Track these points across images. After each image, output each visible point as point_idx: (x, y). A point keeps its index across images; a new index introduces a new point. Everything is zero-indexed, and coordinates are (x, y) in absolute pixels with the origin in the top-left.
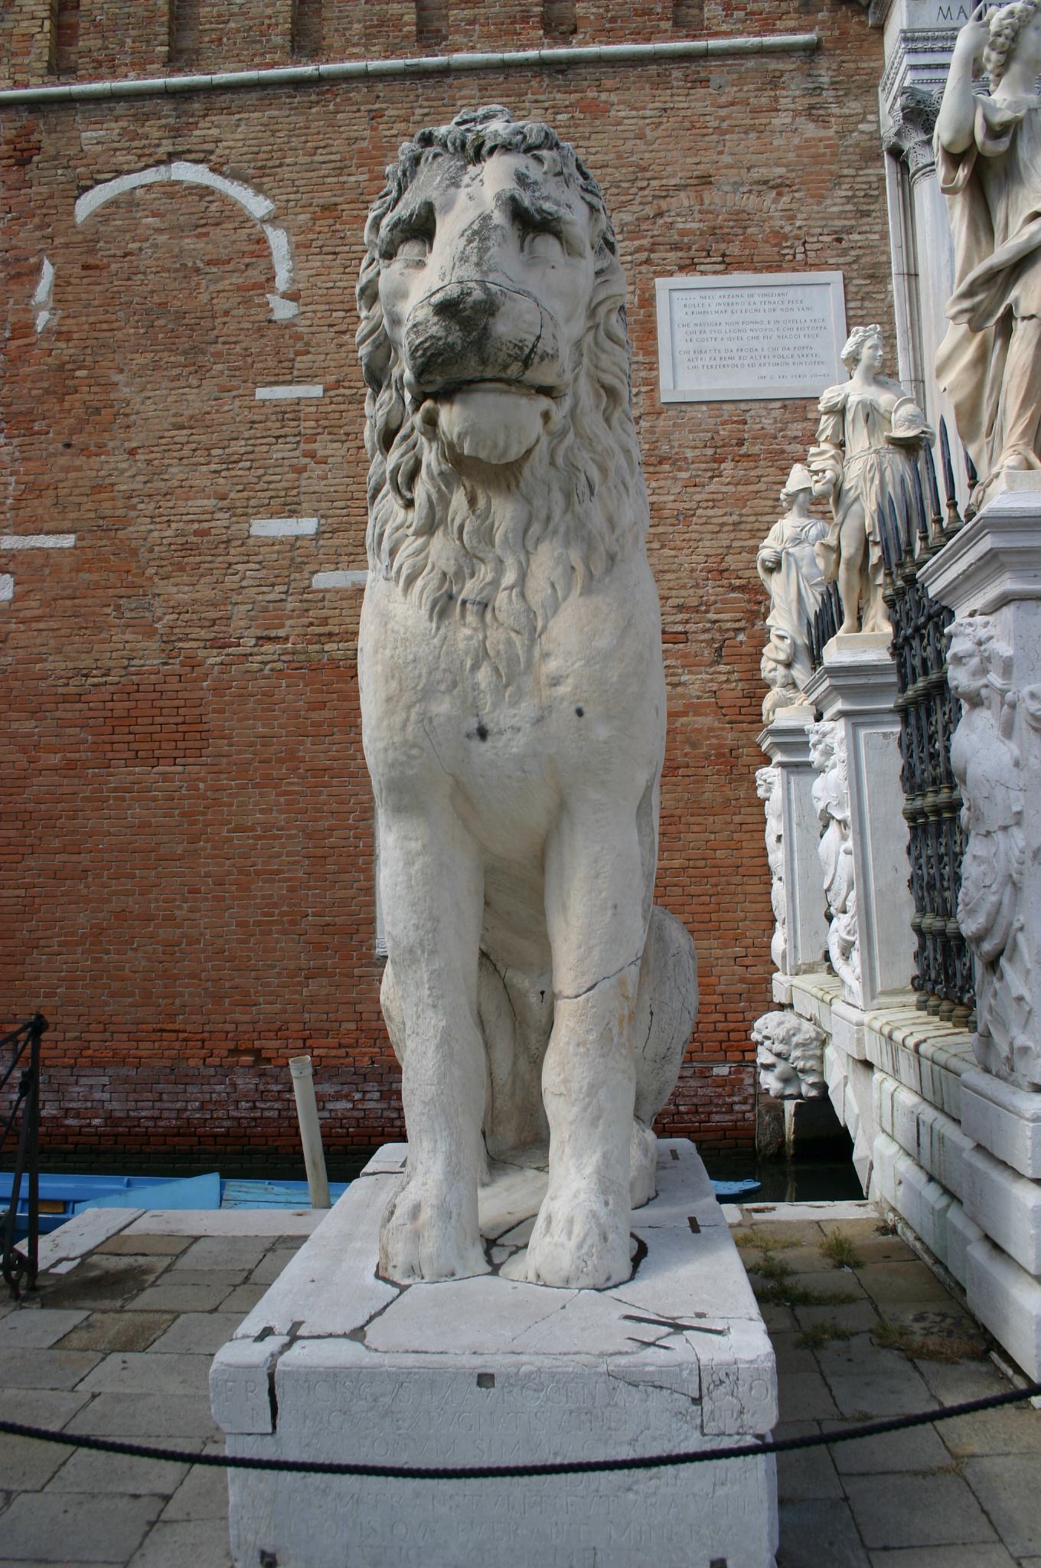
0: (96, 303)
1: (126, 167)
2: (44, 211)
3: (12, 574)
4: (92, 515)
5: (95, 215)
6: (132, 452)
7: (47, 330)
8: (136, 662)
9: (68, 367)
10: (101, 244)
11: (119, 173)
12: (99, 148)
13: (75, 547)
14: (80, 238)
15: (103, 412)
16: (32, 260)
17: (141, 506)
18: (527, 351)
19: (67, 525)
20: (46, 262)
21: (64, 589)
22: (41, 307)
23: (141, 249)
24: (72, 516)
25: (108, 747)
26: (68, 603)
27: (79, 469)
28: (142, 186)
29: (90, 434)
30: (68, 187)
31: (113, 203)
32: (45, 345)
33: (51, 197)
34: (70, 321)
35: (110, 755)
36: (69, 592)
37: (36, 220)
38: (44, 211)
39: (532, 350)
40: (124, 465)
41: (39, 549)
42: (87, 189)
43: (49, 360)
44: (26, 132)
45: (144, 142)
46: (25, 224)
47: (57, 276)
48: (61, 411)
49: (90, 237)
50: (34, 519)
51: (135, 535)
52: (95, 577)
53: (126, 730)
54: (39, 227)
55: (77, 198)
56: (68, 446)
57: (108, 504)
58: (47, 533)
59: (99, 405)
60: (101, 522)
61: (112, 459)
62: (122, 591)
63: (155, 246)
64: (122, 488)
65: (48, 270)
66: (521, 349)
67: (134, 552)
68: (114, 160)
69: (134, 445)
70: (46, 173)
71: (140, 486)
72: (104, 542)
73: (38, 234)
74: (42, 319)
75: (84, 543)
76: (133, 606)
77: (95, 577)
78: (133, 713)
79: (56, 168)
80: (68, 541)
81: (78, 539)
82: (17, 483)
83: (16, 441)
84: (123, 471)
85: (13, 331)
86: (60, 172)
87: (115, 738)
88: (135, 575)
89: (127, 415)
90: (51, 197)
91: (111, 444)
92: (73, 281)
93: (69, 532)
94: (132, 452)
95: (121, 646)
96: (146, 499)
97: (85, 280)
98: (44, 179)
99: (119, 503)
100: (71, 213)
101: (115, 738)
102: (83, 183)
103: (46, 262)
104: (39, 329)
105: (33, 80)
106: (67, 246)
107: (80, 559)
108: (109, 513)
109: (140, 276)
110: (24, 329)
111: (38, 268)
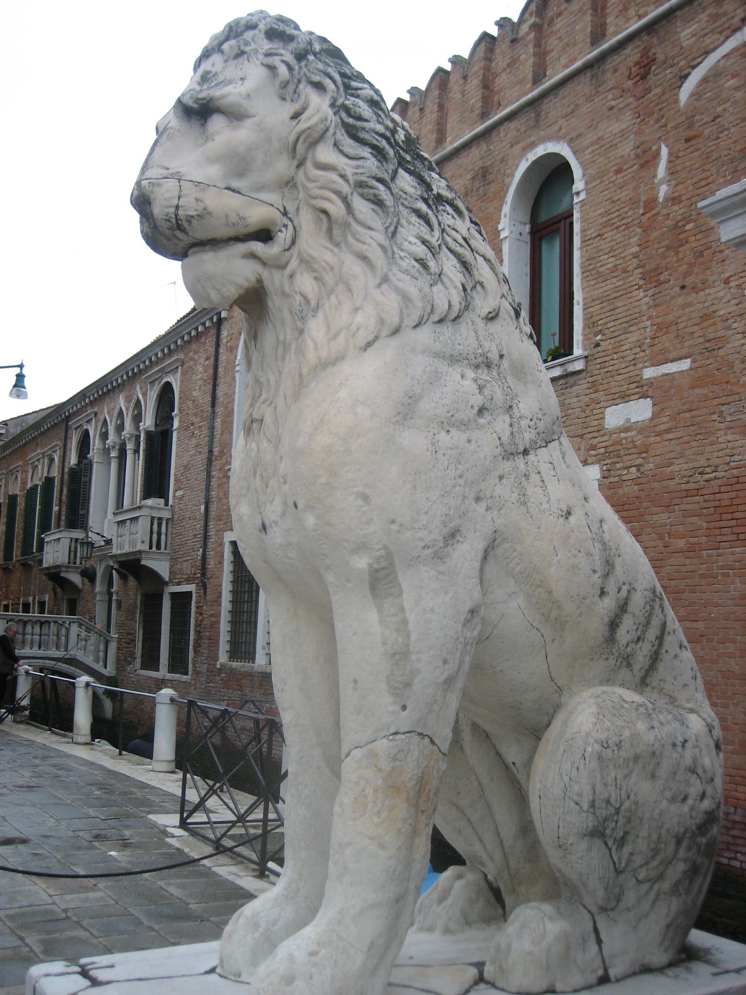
0: (697, 166)
1: (712, 46)
2: (660, 107)
3: (652, 397)
4: (702, 340)
5: (692, 95)
6: (727, 281)
7: (666, 199)
8: (736, 458)
9: (680, 224)
10: (698, 117)
11: (707, 53)
12: (694, 39)
13: (691, 369)
14: (682, 118)
15: (705, 254)
16: (654, 148)
17: (735, 325)
18: (174, 221)
19: (685, 351)
20: (663, 146)
21: (684, 404)
22: (661, 183)
23: (725, 110)
24: (687, 344)
25: (717, 532)
26: (687, 415)
27: (690, 305)
28: (724, 57)
29: (697, 274)
30: (673, 81)
31: (705, 80)
32: (665, 211)
33: (663, 93)
34: (680, 187)
35: (719, 538)
36: (686, 407)
37: (655, 116)
38: (660, 107)
39: (177, 220)
40: (721, 294)
41: (667, 375)
42: (686, 77)
43: (668, 223)
44: (646, 52)
45: (724, 19)
46: (649, 122)
47: (670, 154)
48: (678, 261)
49: (690, 114)
50: (664, 351)
51: (732, 351)
52: (704, 391)
53: (730, 516)
54: (658, 121)
55: (680, 87)
56: (683, 287)
57: (712, 329)
58: (672, 361)
59: (700, 248)
60: (707, 345)
61: (713, 290)
62: (725, 400)
63: (735, 102)
64: (721, 313)
65: (664, 151)
66: (169, 221)
67: (731, 365)
68: (704, 45)
69: (727, 275)
70: (659, 76)
71: (734, 308)
72: (711, 361)
73: (657, 126)
74: (663, 191)
75: (696, 365)
76: (732, 410)
77: (704, 391)
78: (735, 502)
79: (666, 69)
80: (685, 365)
81: (693, 362)
82: (652, 325)
83: (650, 293)
84: (722, 298)
85: (645, 207)
86: (668, 72)
87: (722, 524)
88: (733, 384)
89: (721, 252)
90: (663, 93)
91: (711, 279)
92: (681, 154)
93: (686, 358)
94: (727, 281)
95: (724, 446)
96: (738, 319)
97: (689, 150)
98: (660, 77)
99: (719, 327)
100: (677, 101)
101: (722, 524)
102: (684, 73)
103: (663, 146)
104: (661, 200)
105: (650, 9)
106: (675, 127)
107: (697, 378)
108: (712, 336)
109: (726, 133)
110: (650, 204)
111: (658, 153)
